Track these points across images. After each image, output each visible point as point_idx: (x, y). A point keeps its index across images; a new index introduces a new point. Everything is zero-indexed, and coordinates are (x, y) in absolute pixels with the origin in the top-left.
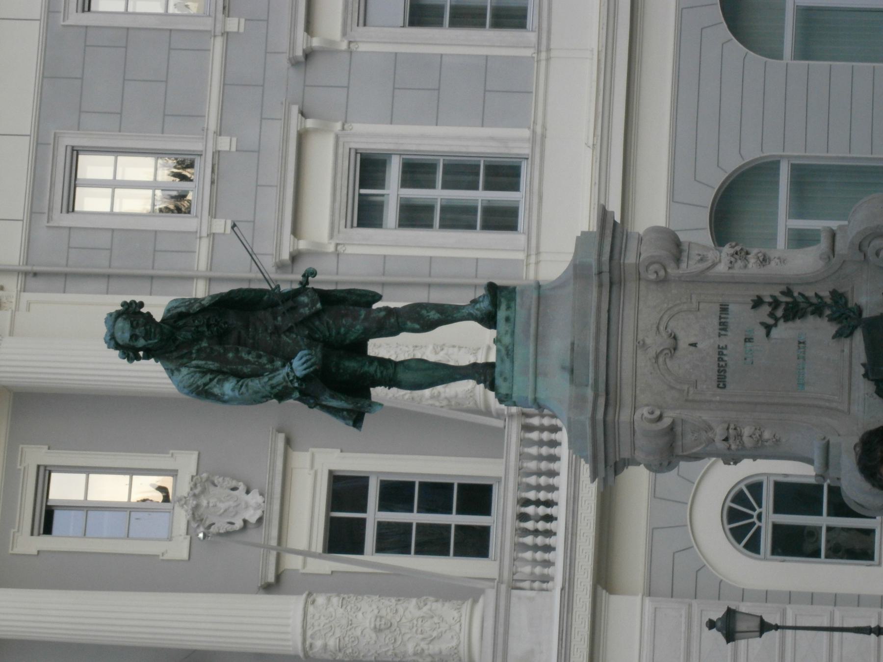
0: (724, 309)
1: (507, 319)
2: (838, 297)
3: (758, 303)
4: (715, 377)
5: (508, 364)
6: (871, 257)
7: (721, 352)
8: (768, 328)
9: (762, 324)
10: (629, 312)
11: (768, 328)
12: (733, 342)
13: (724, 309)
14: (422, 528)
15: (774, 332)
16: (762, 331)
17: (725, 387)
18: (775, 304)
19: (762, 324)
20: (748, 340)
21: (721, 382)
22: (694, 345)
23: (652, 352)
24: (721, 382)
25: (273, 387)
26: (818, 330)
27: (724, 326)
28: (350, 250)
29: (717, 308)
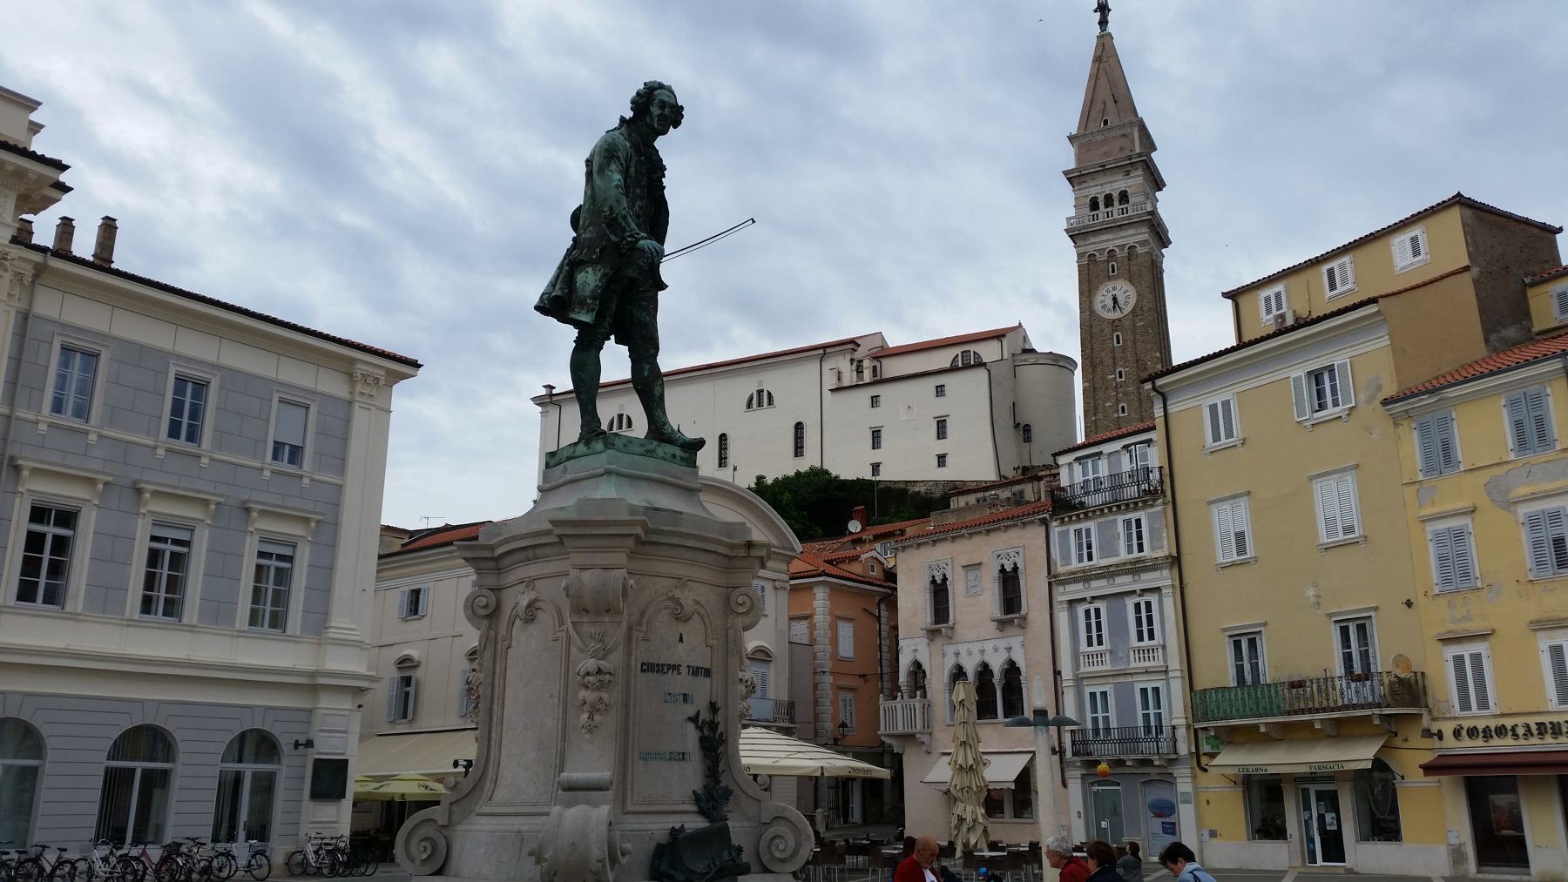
0: (707, 673)
1: (674, 456)
2: (727, 793)
3: (713, 708)
4: (652, 661)
5: (642, 450)
6: (770, 832)
7: (675, 668)
8: (694, 719)
9: (698, 713)
10: (703, 574)
11: (694, 719)
12: (681, 682)
13: (707, 673)
14: (190, 418)
15: (691, 726)
16: (692, 713)
17: (643, 671)
18: (713, 726)
19: (698, 713)
20: (686, 698)
21: (648, 668)
22: (681, 640)
23: (678, 594)
24: (648, 668)
25: (624, 217)
26: (690, 777)
27: (695, 671)
28: (17, 501)
29: (708, 666)
